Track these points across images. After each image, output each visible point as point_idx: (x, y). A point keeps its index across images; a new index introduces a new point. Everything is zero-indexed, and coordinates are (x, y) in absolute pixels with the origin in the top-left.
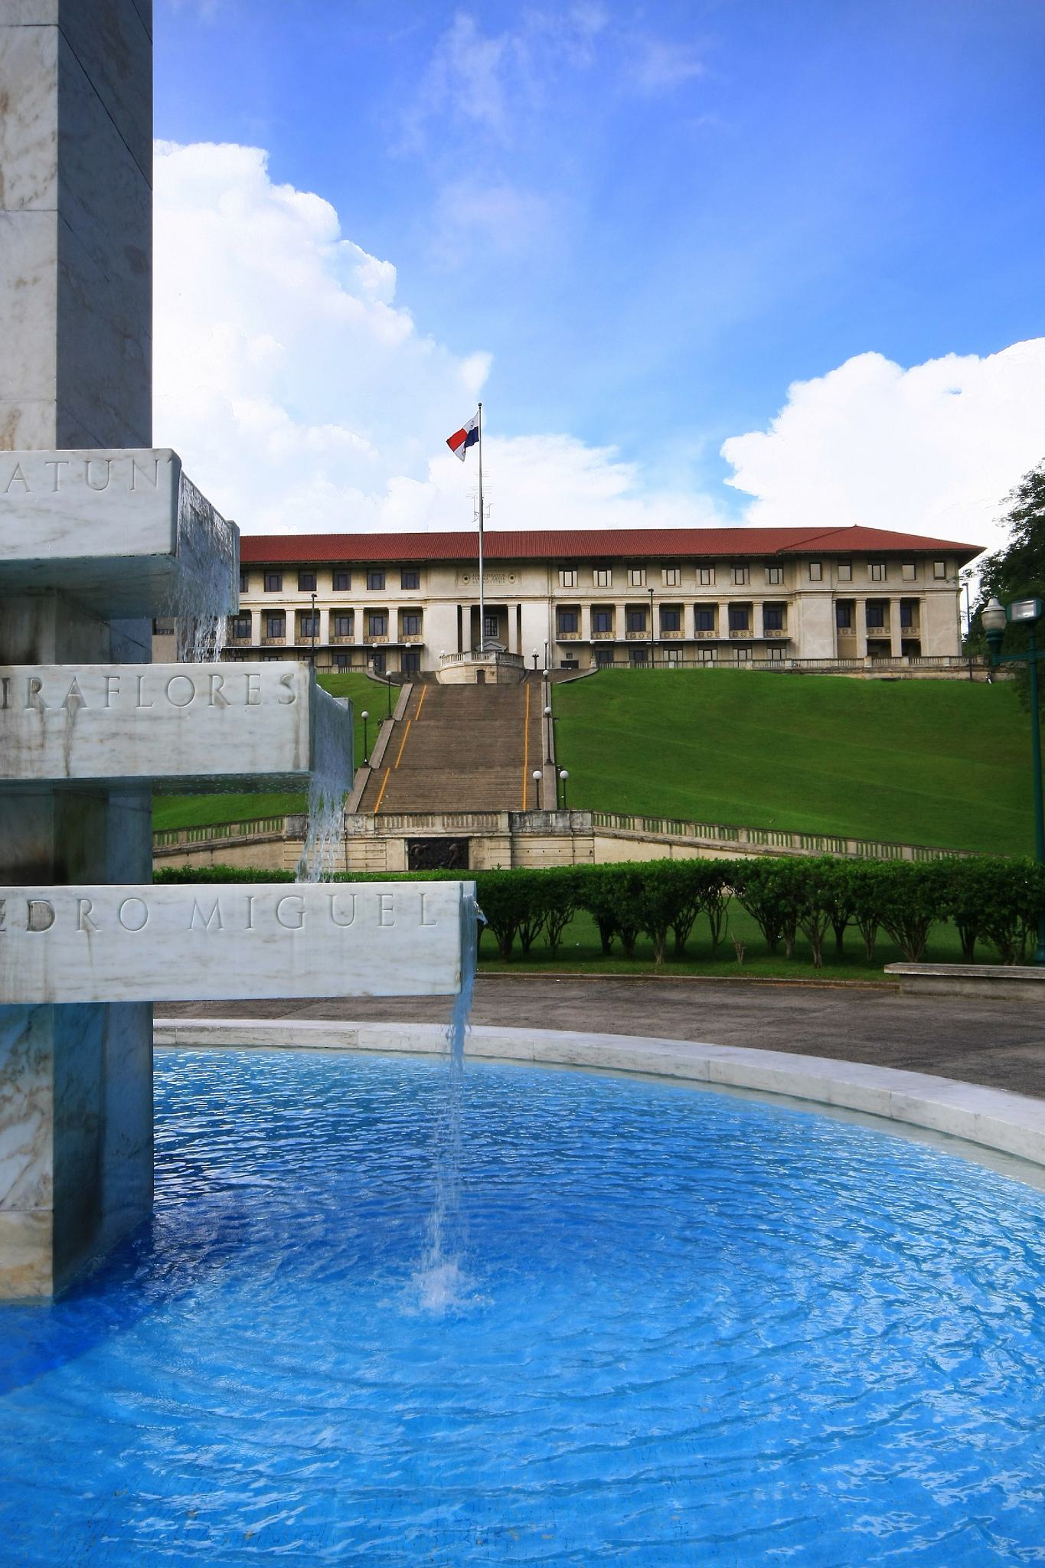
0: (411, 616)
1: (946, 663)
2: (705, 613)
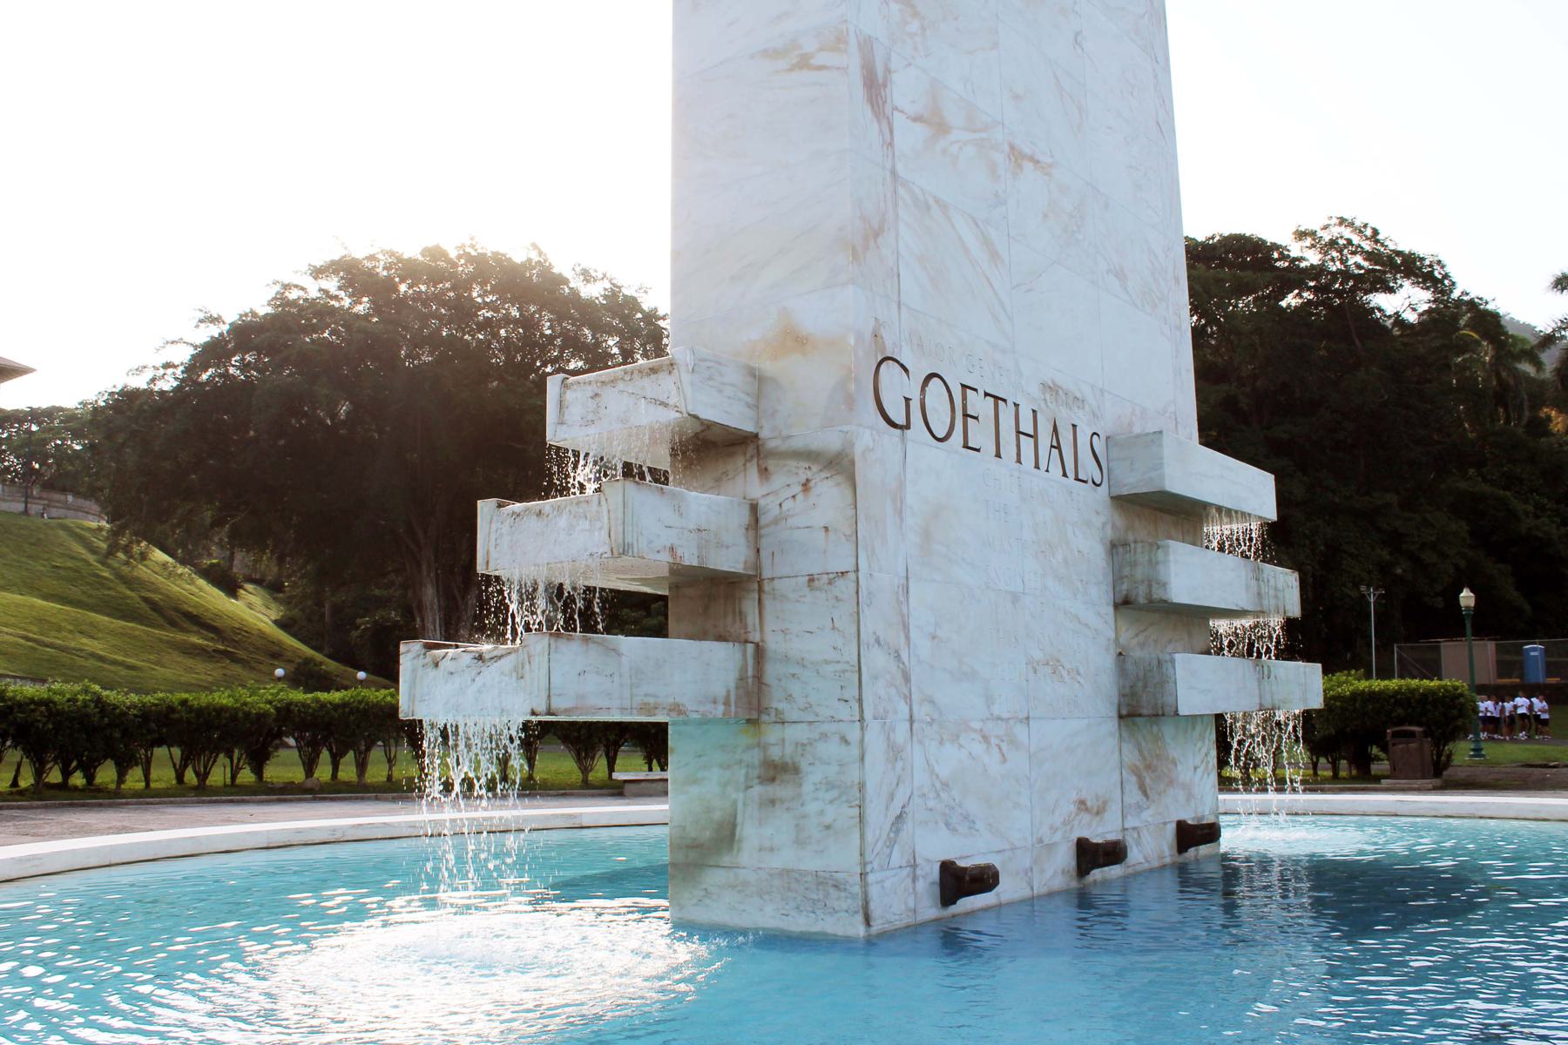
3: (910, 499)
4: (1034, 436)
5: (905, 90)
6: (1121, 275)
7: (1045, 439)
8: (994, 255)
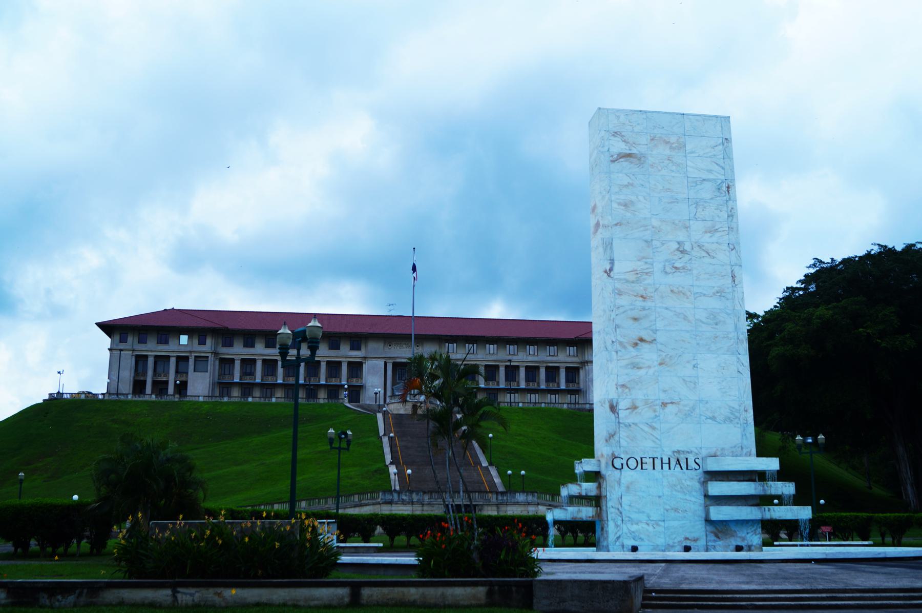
0: (356, 368)
2: (532, 372)
3: (623, 481)
5: (623, 405)
6: (713, 418)
7: (673, 462)
8: (654, 428)
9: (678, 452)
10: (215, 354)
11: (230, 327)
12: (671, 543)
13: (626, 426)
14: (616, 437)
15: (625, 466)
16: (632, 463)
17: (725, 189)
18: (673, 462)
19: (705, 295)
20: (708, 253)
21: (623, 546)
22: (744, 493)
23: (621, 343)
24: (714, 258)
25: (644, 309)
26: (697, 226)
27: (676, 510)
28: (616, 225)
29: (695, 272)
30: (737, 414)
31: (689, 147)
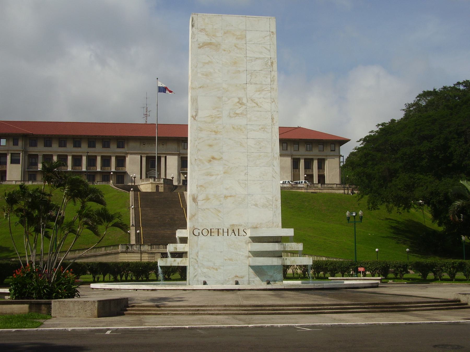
1: (335, 186)
4: (228, 232)
5: (200, 197)
6: (256, 205)
7: (230, 231)
9: (233, 225)
10: (25, 152)
11: (34, 133)
12: (227, 279)
13: (202, 210)
14: (196, 217)
15: (201, 234)
16: (205, 232)
17: (270, 64)
18: (230, 231)
19: (254, 130)
20: (257, 104)
21: (198, 281)
22: (271, 249)
23: (200, 160)
24: (261, 107)
25: (216, 139)
26: (250, 88)
27: (231, 260)
28: (200, 87)
29: (248, 116)
30: (272, 203)
31: (248, 37)
